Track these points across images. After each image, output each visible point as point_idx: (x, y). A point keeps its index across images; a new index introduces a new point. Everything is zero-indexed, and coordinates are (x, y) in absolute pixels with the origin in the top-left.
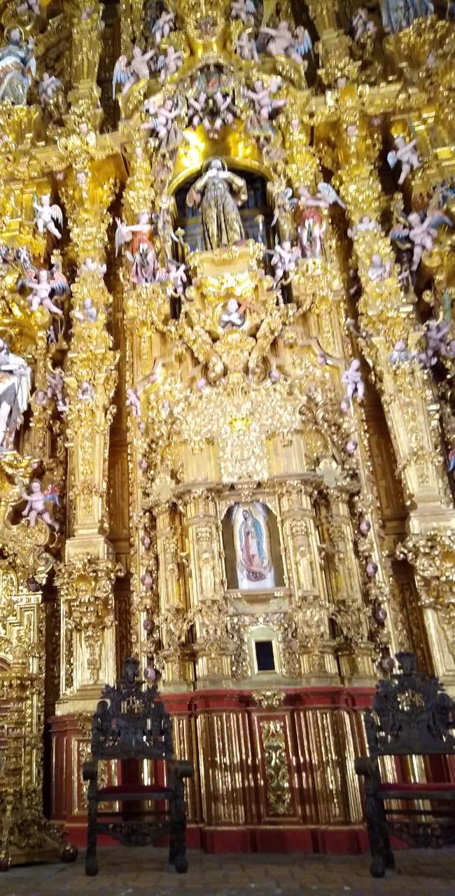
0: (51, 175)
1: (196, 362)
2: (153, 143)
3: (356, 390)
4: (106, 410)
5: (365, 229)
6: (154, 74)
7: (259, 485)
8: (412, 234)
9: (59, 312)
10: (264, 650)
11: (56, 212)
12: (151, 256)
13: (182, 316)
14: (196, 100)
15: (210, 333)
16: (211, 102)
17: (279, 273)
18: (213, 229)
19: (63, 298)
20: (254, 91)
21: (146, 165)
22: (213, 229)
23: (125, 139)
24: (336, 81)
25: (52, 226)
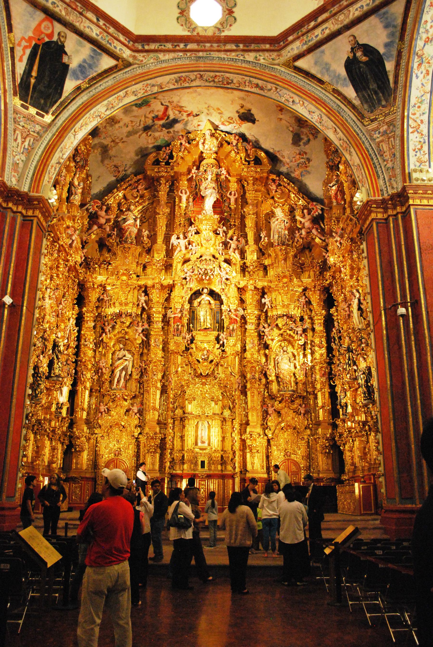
0: (146, 287)
5: (250, 327)
9: (145, 339)
10: (203, 463)
12: (180, 327)
17: (221, 342)
19: (147, 334)
20: (221, 271)
25: (144, 305)
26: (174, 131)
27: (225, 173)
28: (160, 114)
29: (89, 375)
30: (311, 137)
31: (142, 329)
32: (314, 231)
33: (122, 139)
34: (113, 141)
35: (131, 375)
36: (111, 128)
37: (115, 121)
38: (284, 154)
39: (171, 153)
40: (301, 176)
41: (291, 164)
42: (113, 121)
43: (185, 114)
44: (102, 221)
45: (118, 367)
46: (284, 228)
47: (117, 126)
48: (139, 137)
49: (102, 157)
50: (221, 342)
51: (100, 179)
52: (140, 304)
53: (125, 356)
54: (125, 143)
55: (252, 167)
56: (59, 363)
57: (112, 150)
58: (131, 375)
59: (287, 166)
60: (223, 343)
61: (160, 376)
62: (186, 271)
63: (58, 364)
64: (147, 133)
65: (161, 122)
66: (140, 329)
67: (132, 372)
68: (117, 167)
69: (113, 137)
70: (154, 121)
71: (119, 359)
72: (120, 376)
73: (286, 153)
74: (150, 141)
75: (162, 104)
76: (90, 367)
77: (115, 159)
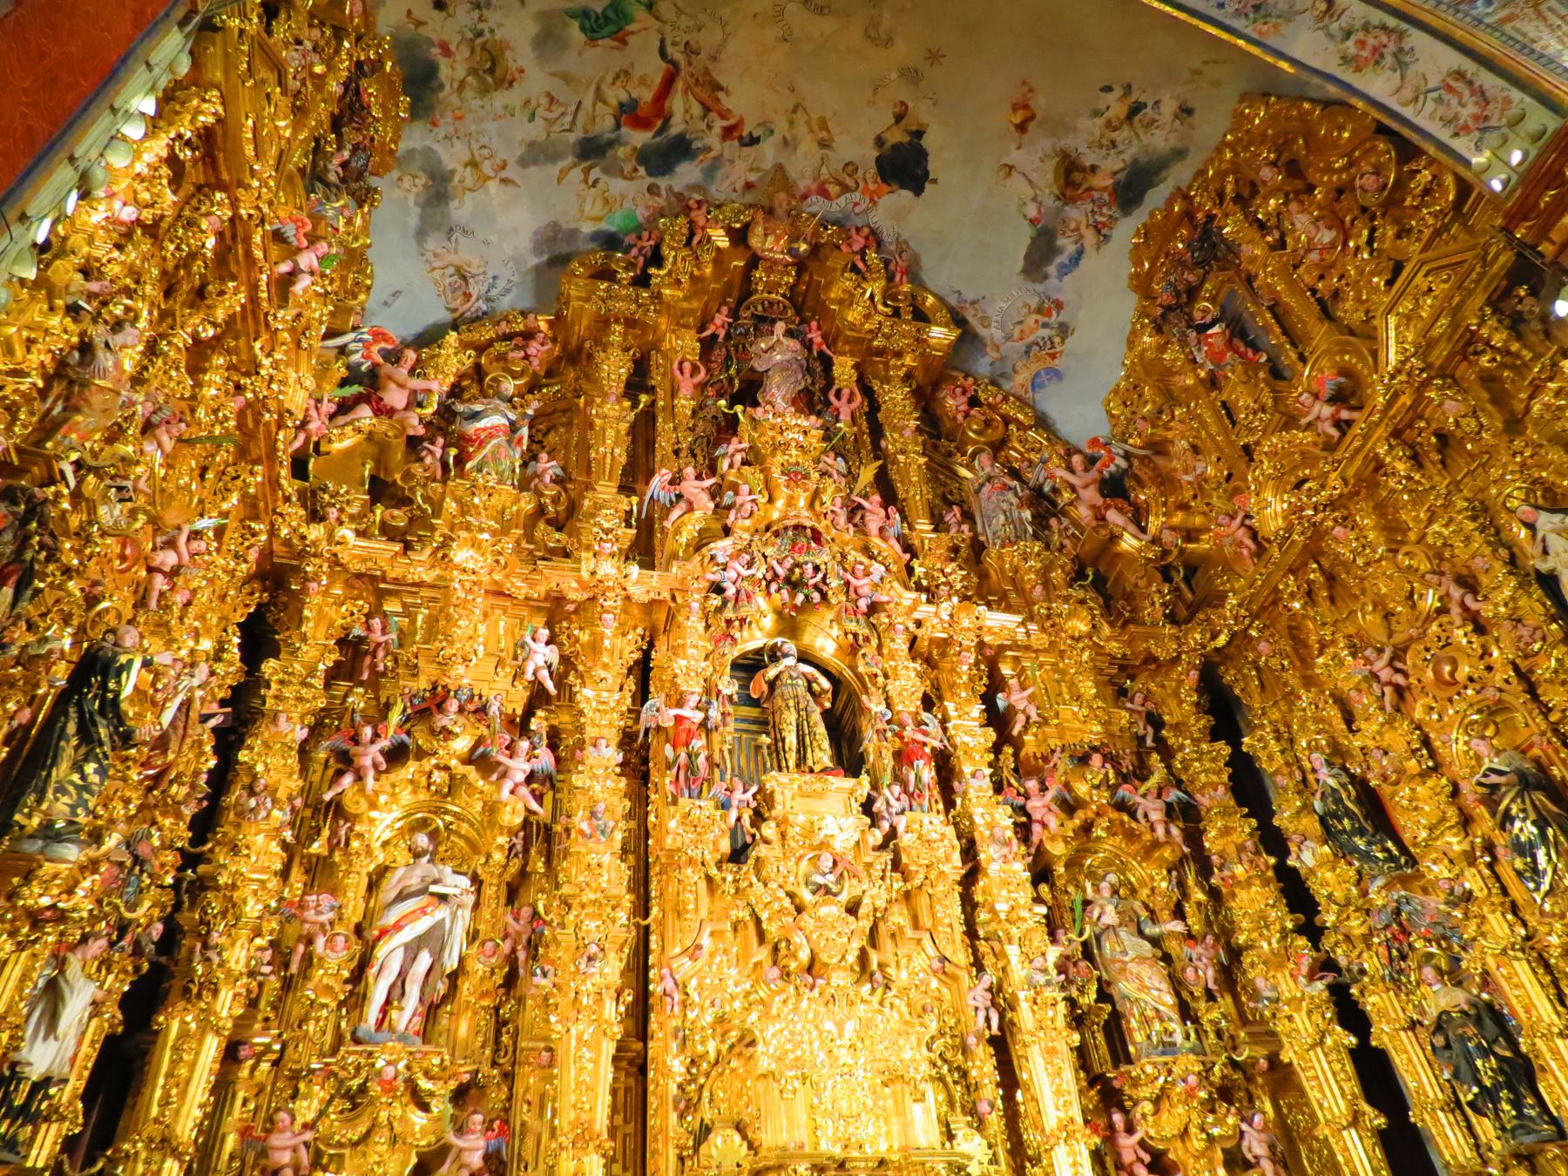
1: (761, 936)
2: (716, 601)
3: (988, 1020)
4: (619, 994)
6: (721, 510)
7: (882, 1163)
8: (1030, 805)
11: (551, 654)
13: (751, 862)
14: (780, 563)
15: (791, 895)
16: (797, 571)
18: (791, 740)
21: (701, 626)
22: (791, 740)
23: (677, 585)
24: (937, 586)
25: (545, 673)
26: (670, 189)
27: (818, 340)
28: (647, 96)
29: (238, 956)
30: (1090, 237)
31: (527, 767)
32: (1113, 516)
33: (504, 166)
34: (473, 164)
35: (454, 977)
36: (478, 102)
37: (498, 72)
38: (989, 313)
39: (657, 249)
40: (1033, 389)
41: (1006, 348)
42: (491, 71)
43: (719, 124)
44: (395, 397)
45: (398, 927)
46: (1015, 501)
47: (500, 99)
48: (559, 180)
49: (422, 217)
50: (886, 826)
51: (399, 302)
52: (530, 669)
53: (435, 882)
54: (511, 189)
55: (907, 322)
56: (90, 768)
57: (462, 202)
58: (454, 977)
59: (995, 355)
60: (893, 829)
61: (612, 969)
62: (721, 559)
63: (78, 767)
64: (587, 171)
65: (640, 138)
66: (519, 768)
67: (461, 960)
68: (464, 278)
69: (475, 146)
70: (618, 126)
71: (401, 897)
72: (402, 976)
73: (994, 310)
74: (588, 208)
75: (663, 53)
76: (252, 909)
77: (462, 240)
